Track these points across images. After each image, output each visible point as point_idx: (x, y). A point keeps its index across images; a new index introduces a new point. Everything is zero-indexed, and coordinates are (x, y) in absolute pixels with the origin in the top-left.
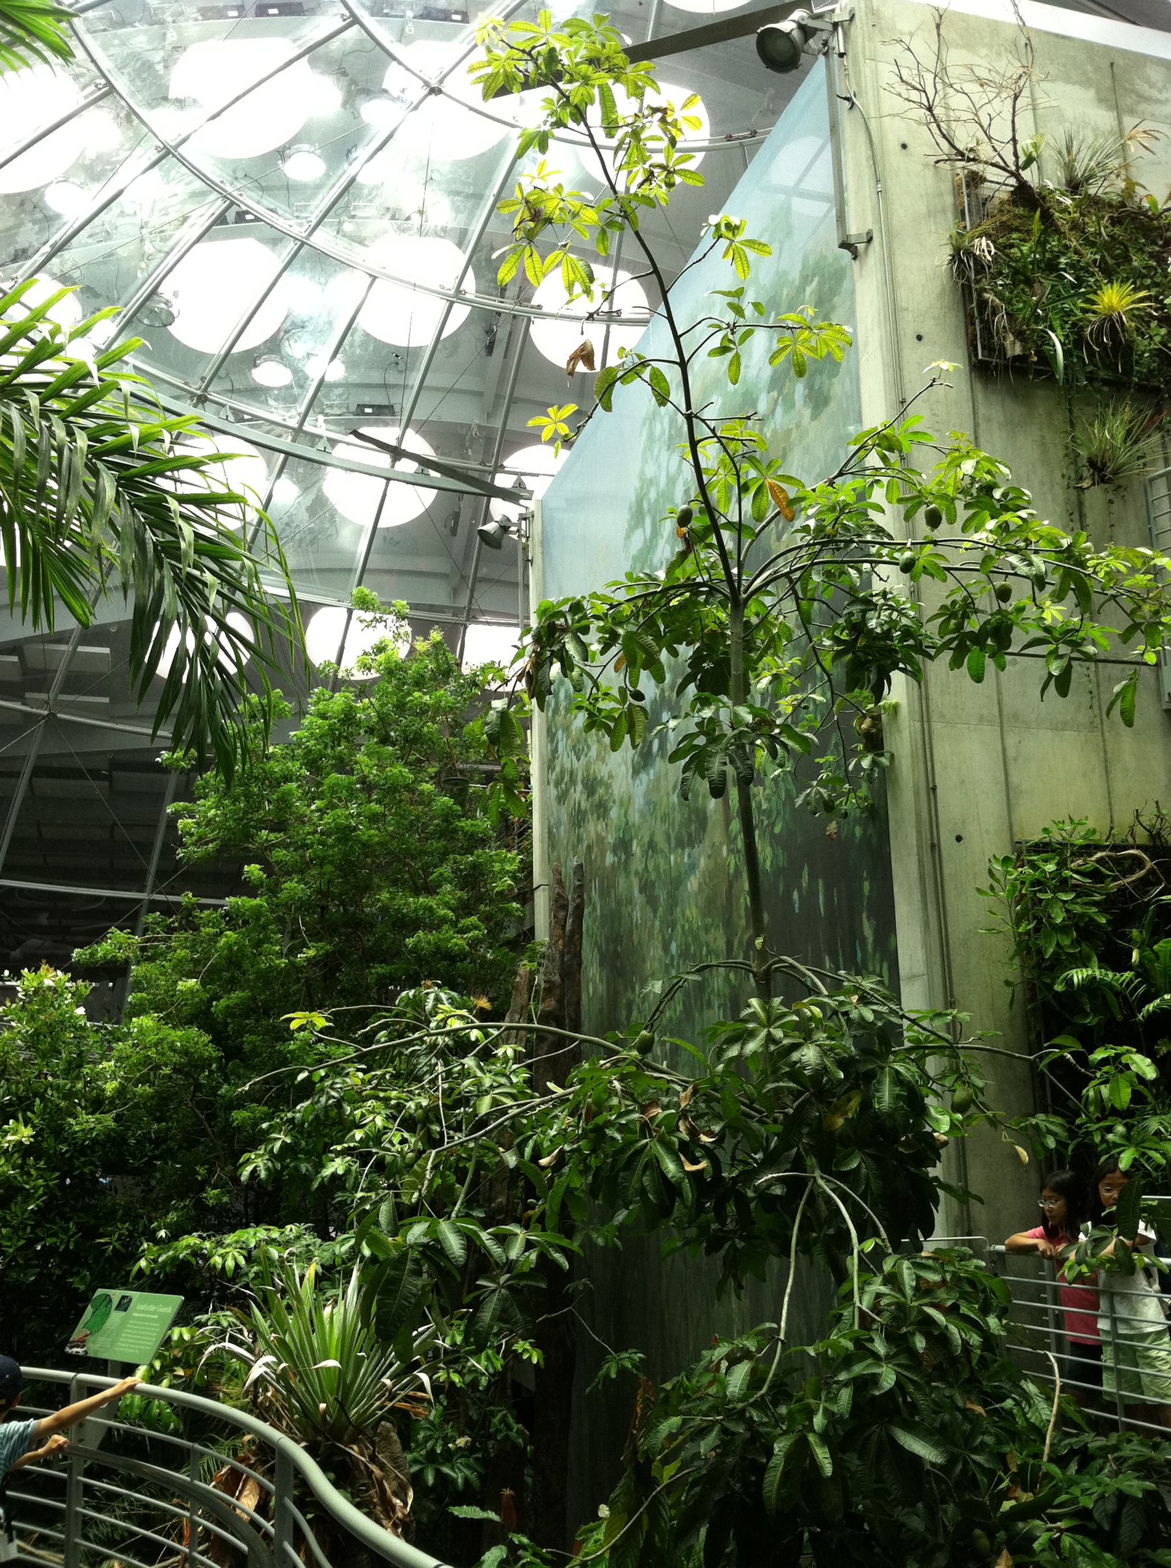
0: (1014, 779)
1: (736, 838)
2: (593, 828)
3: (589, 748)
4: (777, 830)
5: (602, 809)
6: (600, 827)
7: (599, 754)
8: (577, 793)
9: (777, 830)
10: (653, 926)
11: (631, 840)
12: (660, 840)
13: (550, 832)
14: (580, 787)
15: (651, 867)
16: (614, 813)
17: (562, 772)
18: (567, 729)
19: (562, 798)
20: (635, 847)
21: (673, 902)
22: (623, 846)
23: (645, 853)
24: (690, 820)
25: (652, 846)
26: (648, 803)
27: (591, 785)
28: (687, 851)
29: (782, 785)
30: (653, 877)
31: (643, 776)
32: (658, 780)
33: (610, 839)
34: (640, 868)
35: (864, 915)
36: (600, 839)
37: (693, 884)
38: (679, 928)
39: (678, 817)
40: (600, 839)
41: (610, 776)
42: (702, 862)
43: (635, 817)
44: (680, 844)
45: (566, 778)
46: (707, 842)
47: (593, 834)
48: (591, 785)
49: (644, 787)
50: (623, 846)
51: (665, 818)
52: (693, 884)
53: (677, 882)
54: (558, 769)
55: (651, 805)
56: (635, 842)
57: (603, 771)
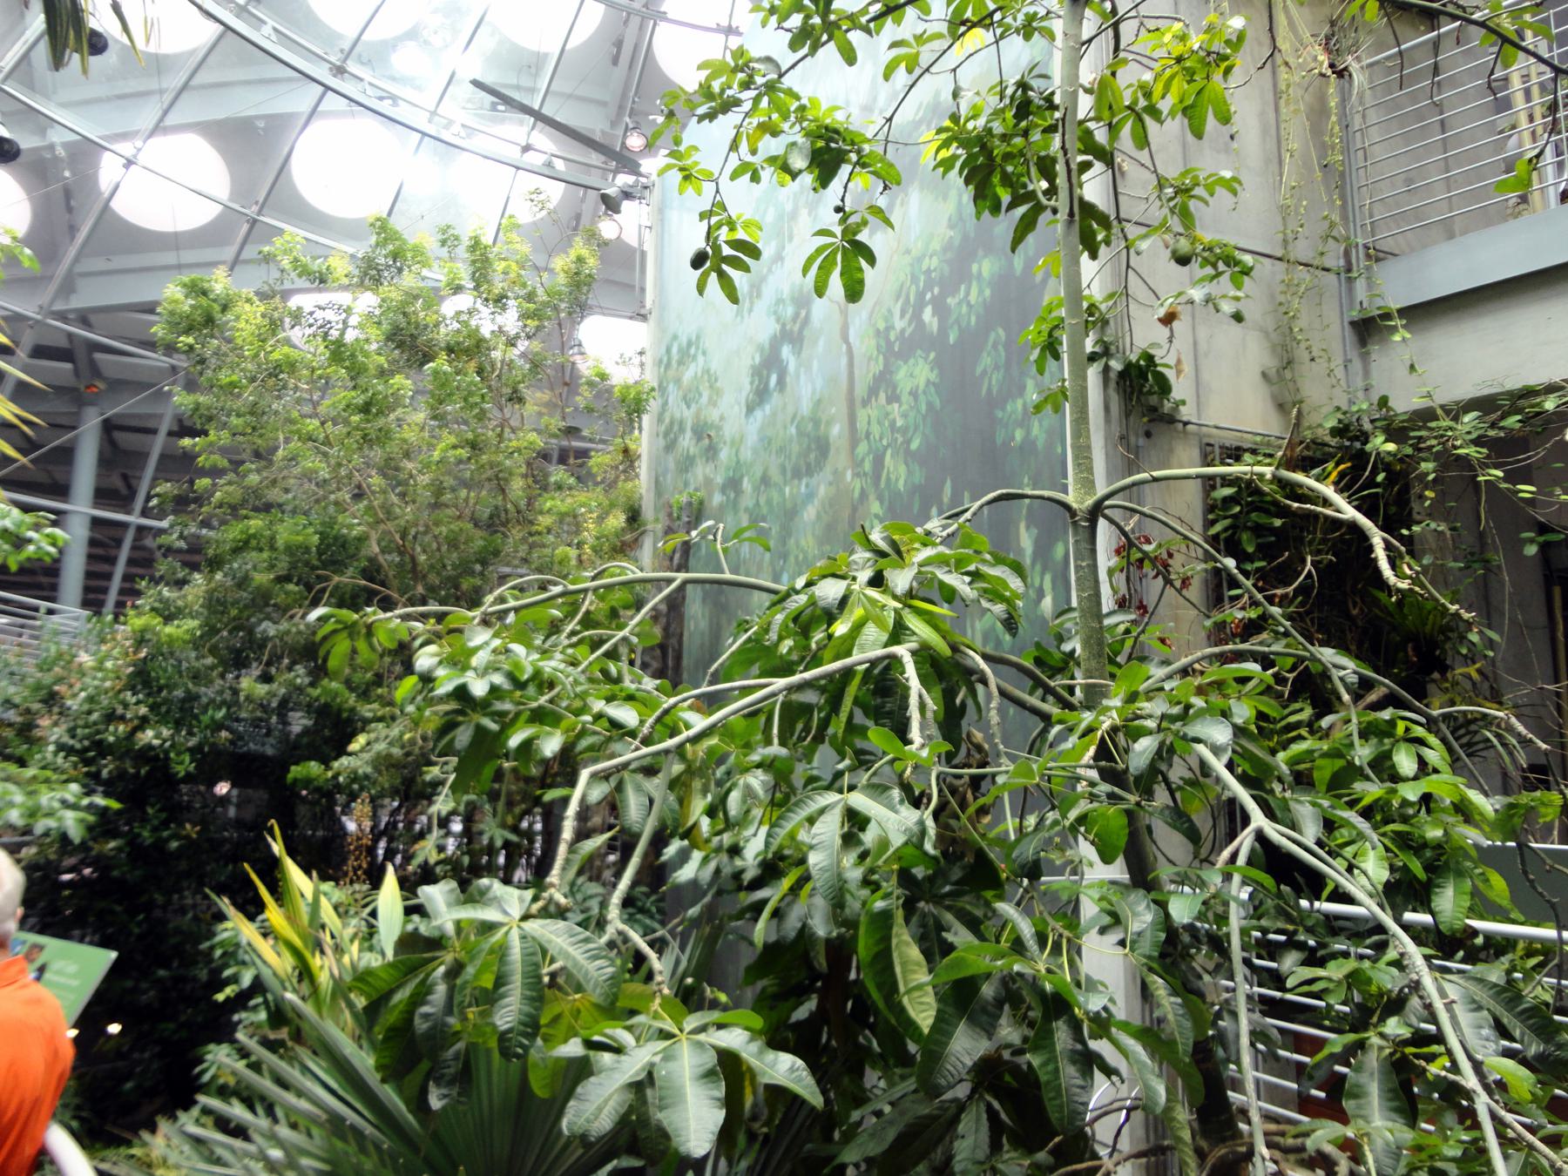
0: (1205, 376)
1: (863, 460)
2: (701, 471)
3: (700, 395)
4: (914, 445)
5: (711, 452)
6: (709, 469)
7: (710, 399)
8: (687, 442)
9: (914, 445)
10: (762, 560)
11: (742, 477)
12: (775, 475)
13: (657, 482)
14: (689, 434)
15: (762, 501)
16: (724, 455)
17: (672, 423)
18: (678, 381)
19: (670, 447)
20: (746, 485)
21: (786, 533)
22: (733, 484)
23: (756, 489)
24: (809, 448)
25: (765, 480)
26: (761, 440)
27: (700, 432)
28: (804, 481)
29: (922, 398)
30: (765, 511)
31: (758, 414)
32: (774, 414)
33: (719, 480)
34: (750, 504)
35: (1022, 526)
36: (708, 482)
37: (810, 513)
38: (792, 559)
39: (795, 448)
40: (708, 482)
41: (722, 418)
42: (822, 490)
43: (746, 454)
44: (797, 474)
45: (676, 428)
46: (828, 469)
47: (700, 477)
48: (700, 432)
49: (758, 425)
50: (733, 484)
51: (781, 450)
52: (810, 513)
53: (790, 514)
54: (667, 420)
55: (766, 441)
56: (746, 480)
57: (713, 415)
